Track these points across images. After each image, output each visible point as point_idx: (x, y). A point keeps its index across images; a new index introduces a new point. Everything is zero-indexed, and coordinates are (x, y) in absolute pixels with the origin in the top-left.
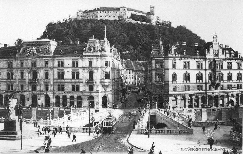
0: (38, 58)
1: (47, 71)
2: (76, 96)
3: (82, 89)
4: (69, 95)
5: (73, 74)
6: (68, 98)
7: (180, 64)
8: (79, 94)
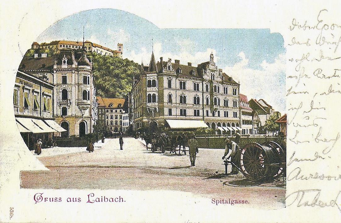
7: (175, 83)
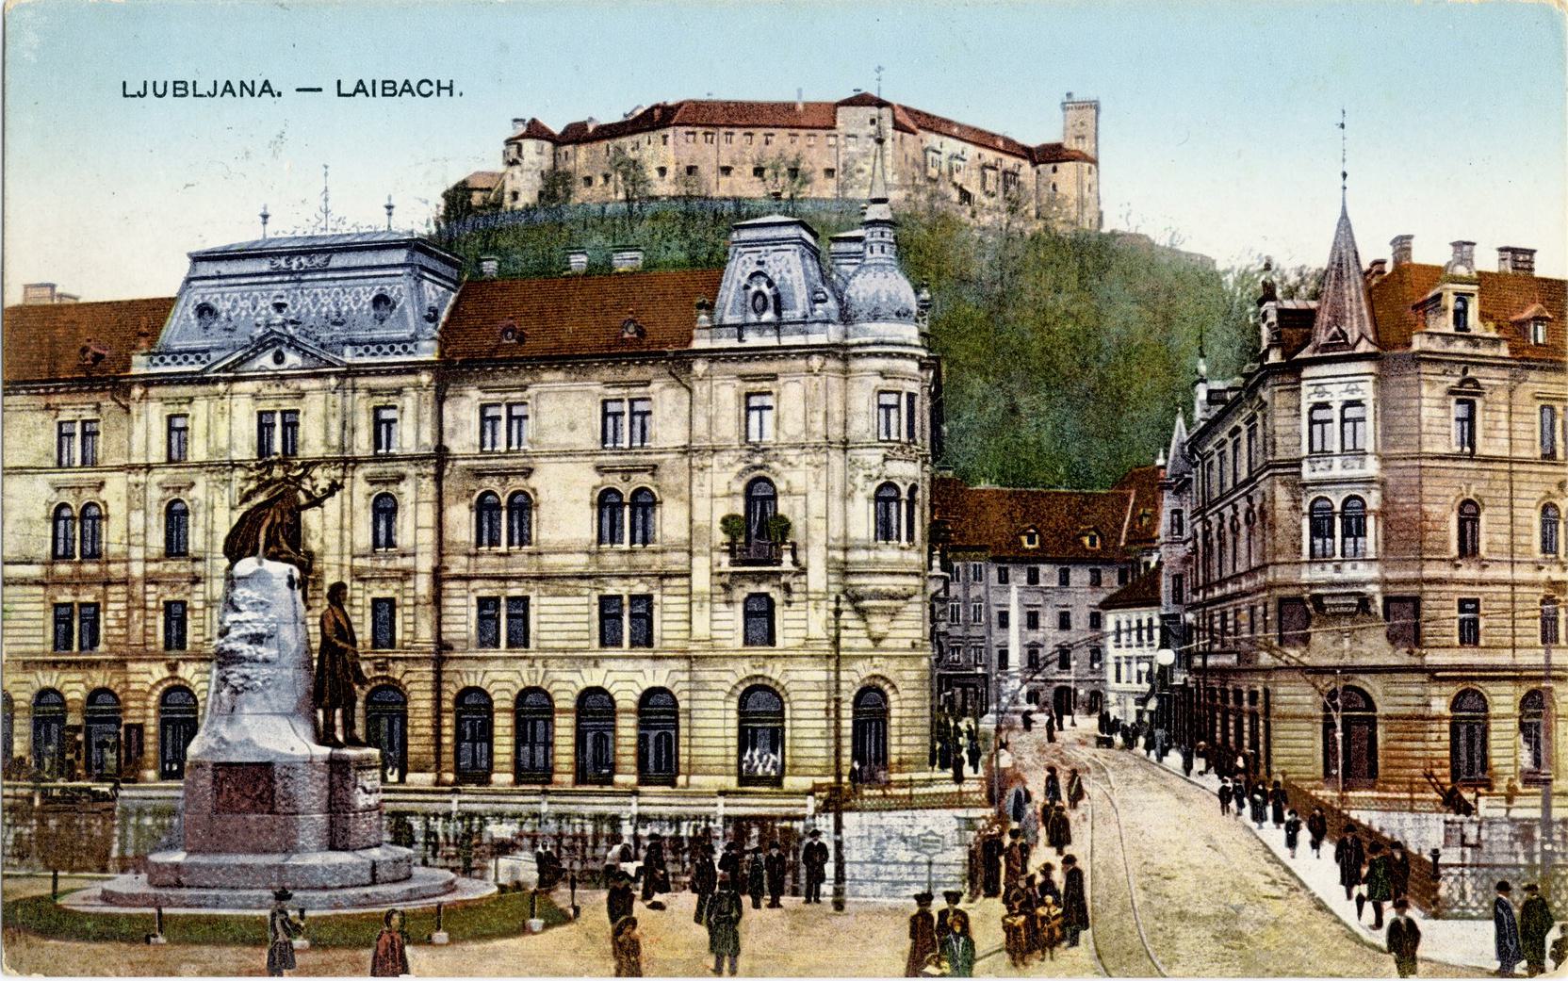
0: (316, 384)
1: (392, 489)
2: (626, 697)
3: (685, 617)
4: (566, 686)
5: (607, 503)
6: (562, 711)
8: (656, 676)
